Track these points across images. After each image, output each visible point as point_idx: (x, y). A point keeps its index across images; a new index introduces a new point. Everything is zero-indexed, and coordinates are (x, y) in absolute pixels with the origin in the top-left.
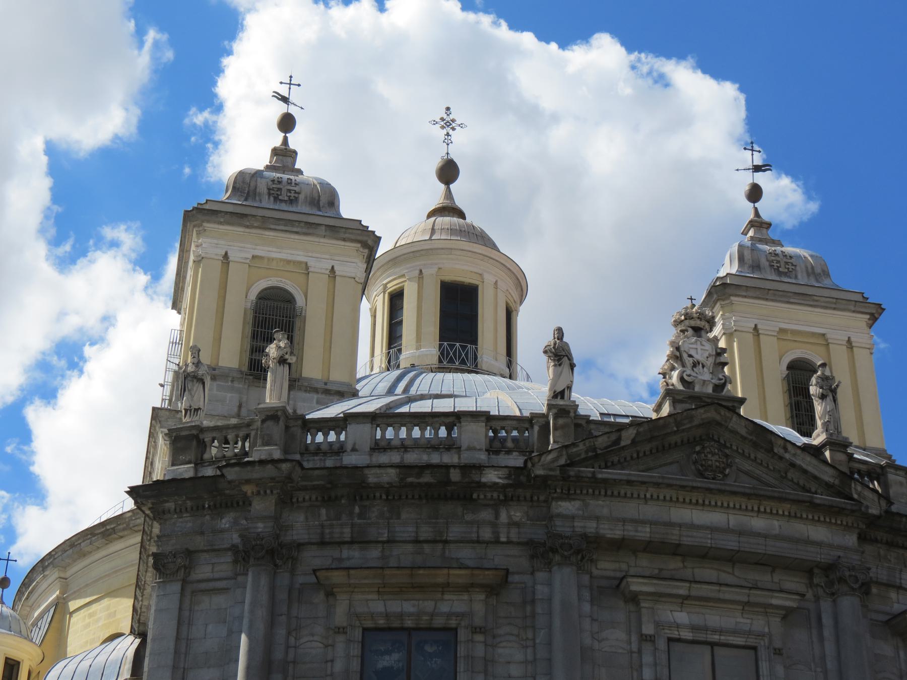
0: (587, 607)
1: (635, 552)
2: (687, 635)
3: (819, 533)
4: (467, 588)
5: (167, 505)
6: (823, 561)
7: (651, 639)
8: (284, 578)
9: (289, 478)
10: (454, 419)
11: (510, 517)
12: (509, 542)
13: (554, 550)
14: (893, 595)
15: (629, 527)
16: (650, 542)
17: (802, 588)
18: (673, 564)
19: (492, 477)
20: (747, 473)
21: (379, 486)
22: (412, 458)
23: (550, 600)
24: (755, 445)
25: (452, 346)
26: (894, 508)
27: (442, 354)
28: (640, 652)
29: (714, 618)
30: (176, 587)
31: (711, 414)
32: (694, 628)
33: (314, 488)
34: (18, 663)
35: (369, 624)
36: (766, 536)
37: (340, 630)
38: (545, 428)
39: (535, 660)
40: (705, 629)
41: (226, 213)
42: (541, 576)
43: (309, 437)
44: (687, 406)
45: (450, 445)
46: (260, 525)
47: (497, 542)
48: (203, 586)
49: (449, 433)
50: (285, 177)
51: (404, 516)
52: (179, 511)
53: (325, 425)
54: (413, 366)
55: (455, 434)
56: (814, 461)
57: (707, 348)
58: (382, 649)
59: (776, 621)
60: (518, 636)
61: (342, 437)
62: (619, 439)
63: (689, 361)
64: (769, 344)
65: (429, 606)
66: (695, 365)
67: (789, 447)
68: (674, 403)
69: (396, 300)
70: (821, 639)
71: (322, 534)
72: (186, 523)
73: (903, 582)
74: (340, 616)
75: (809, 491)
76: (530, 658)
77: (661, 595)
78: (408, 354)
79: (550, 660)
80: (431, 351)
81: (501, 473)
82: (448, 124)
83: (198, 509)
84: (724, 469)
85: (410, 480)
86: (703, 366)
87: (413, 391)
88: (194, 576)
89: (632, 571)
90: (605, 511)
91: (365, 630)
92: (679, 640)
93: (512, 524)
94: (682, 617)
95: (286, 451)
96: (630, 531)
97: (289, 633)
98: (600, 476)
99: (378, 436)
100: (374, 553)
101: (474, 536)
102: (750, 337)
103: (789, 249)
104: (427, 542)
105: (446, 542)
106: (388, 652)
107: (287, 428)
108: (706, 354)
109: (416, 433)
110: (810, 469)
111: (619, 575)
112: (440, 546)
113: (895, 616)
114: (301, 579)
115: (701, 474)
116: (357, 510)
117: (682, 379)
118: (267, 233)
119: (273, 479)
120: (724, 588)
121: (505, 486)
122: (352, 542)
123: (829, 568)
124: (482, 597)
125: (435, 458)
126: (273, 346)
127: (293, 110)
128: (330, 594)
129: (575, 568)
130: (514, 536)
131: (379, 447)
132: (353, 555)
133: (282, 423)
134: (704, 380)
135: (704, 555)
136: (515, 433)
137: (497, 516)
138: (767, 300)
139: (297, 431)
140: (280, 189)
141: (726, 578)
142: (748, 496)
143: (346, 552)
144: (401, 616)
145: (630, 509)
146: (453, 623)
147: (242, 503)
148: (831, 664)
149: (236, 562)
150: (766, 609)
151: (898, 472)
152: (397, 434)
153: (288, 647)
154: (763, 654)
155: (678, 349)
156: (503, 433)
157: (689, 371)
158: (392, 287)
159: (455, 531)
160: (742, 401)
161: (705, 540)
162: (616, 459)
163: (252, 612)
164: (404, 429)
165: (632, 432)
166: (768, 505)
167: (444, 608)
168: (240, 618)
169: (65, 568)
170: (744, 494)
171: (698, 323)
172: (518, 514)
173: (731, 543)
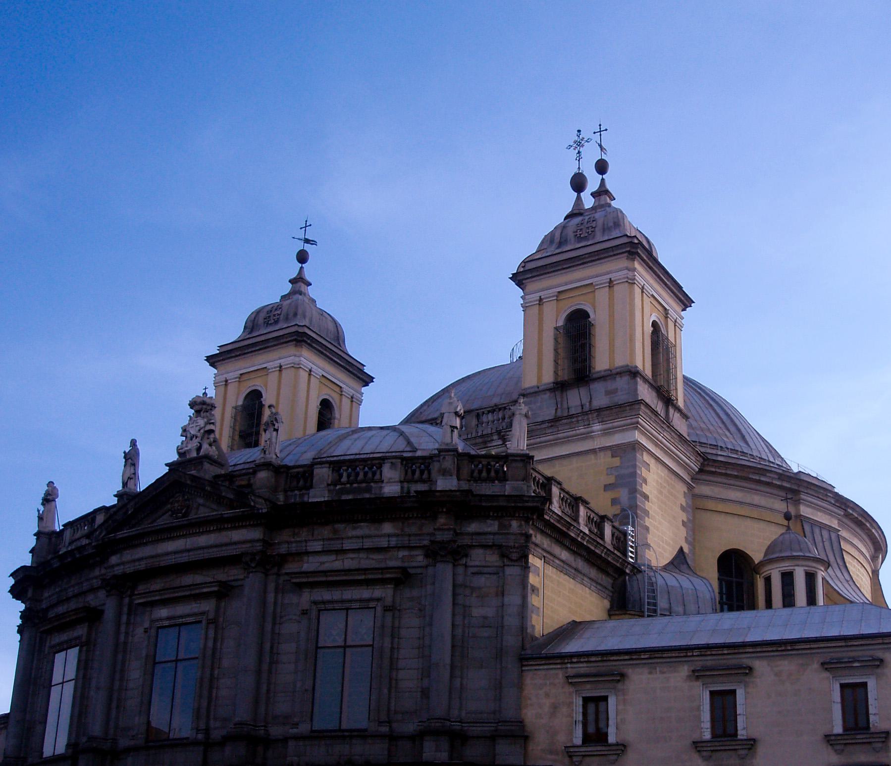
0: (124, 618)
2: (166, 623)
6: (237, 553)
14: (306, 558)
15: (137, 564)
29: (181, 609)
32: (169, 618)
57: (199, 424)
62: (127, 511)
73: (308, 548)
84: (182, 509)
86: (196, 437)
107: (50, 539)
108: (198, 428)
151: (323, 466)
171: (197, 408)
173: (184, 558)
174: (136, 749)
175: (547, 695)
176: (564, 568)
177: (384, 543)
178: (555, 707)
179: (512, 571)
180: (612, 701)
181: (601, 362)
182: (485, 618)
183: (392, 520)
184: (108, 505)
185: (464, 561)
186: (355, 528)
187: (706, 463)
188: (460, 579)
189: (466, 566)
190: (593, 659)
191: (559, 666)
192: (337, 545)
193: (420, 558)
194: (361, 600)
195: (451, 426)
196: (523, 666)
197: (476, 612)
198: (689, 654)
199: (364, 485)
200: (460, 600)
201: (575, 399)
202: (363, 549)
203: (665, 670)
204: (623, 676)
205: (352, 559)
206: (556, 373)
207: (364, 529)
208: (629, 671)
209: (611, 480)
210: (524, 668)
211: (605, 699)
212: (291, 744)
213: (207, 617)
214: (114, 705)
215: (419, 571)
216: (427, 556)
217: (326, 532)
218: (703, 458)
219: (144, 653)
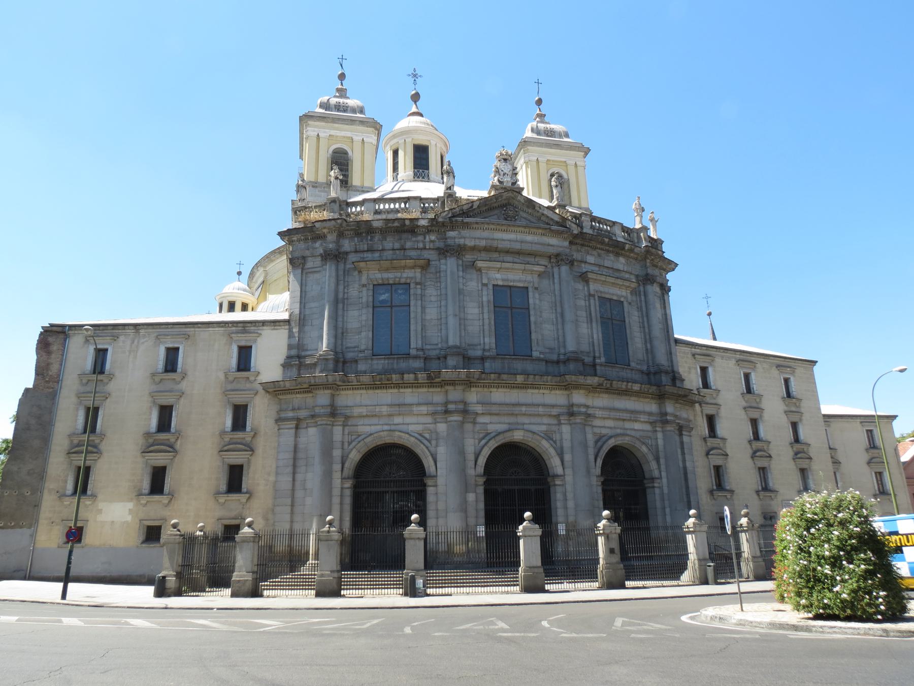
0: (461, 274)
1: (480, 251)
2: (500, 283)
3: (554, 241)
4: (413, 267)
5: (294, 239)
7: (486, 285)
8: (341, 266)
9: (341, 224)
10: (407, 200)
11: (430, 239)
12: (430, 249)
13: (447, 251)
14: (583, 265)
15: (477, 241)
16: (485, 247)
17: (546, 263)
18: (495, 255)
19: (423, 223)
20: (525, 218)
21: (377, 228)
22: (390, 216)
23: (446, 271)
24: (528, 207)
25: (418, 171)
26: (585, 231)
27: (415, 175)
28: (482, 290)
30: (300, 271)
31: (510, 194)
32: (503, 280)
33: (351, 230)
34: (247, 304)
35: (375, 283)
36: (532, 243)
37: (364, 286)
38: (443, 203)
39: (441, 294)
40: (507, 280)
41: (317, 117)
42: (443, 261)
43: (349, 209)
44: (501, 191)
45: (405, 210)
46: (331, 245)
47: (425, 248)
48: (310, 270)
49: (405, 206)
50: (341, 100)
51: (388, 239)
52: (299, 240)
53: (355, 204)
54: (403, 180)
55: (407, 206)
56: (551, 212)
58: (381, 292)
59: (536, 278)
60: (434, 285)
61: (363, 209)
62: (472, 207)
63: (502, 173)
64: (543, 166)
65: (399, 275)
66: (504, 175)
67: (542, 207)
68: (496, 189)
69: (396, 153)
70: (554, 283)
71: (356, 248)
72: (302, 245)
74: (364, 280)
75: (549, 225)
76: (439, 294)
77: (490, 268)
78: (402, 174)
79: (446, 294)
80: (410, 173)
81: (426, 221)
82: (415, 76)
83: (306, 239)
85: (389, 225)
87: (394, 190)
88: (306, 267)
89: (479, 259)
90: (468, 235)
91: (374, 285)
92: (497, 285)
93: (431, 241)
94: (498, 276)
95: (341, 214)
96: (478, 243)
97: (344, 288)
98: (465, 221)
99: (377, 208)
100: (377, 255)
101: (416, 247)
102: (535, 163)
103: (552, 126)
104: (397, 250)
105: (405, 249)
106: (384, 294)
107: (340, 205)
109: (392, 206)
110: (549, 215)
111: (473, 260)
112: (403, 251)
113: (583, 274)
114: (348, 266)
115: (506, 219)
116: (369, 238)
117: (499, 181)
118: (335, 125)
119: (335, 227)
120: (515, 264)
121: (428, 226)
122: (368, 251)
123: (557, 255)
124: (420, 270)
125: (400, 215)
126: (333, 172)
128: (360, 272)
129: (455, 258)
130: (432, 246)
131: (377, 212)
132: (369, 255)
133: (338, 204)
134: (507, 180)
135: (508, 252)
136: (432, 205)
137: (425, 238)
138: (542, 147)
139: (344, 207)
140: (340, 106)
141: (516, 260)
142: (525, 227)
143: (366, 255)
144: (388, 279)
145: (478, 233)
146: (408, 281)
147: (322, 237)
148: (557, 292)
149: (322, 260)
150: (532, 272)
152: (384, 207)
153: (344, 293)
154: (530, 290)
155: (497, 168)
156: (427, 205)
157: (501, 177)
158: (394, 147)
159: (409, 245)
160: (523, 189)
161: (507, 245)
162: (472, 214)
163: (329, 280)
164: (397, 204)
165: (478, 203)
166: (533, 230)
167: (405, 275)
168: (325, 282)
169: (265, 267)
170: (523, 227)
171: (506, 157)
172: (433, 238)
173: (517, 246)
174: (493, 358)
175: (686, 362)
177: (621, 267)
178: (690, 368)
180: (710, 370)
183: (622, 255)
184: (423, 196)
186: (608, 256)
190: (703, 348)
192: (600, 262)
194: (617, 295)
196: (676, 345)
199: (607, 233)
202: (612, 268)
205: (606, 272)
207: (612, 257)
210: (677, 347)
212: (598, 367)
213: (533, 285)
214: (462, 327)
217: (595, 253)
219: (485, 299)
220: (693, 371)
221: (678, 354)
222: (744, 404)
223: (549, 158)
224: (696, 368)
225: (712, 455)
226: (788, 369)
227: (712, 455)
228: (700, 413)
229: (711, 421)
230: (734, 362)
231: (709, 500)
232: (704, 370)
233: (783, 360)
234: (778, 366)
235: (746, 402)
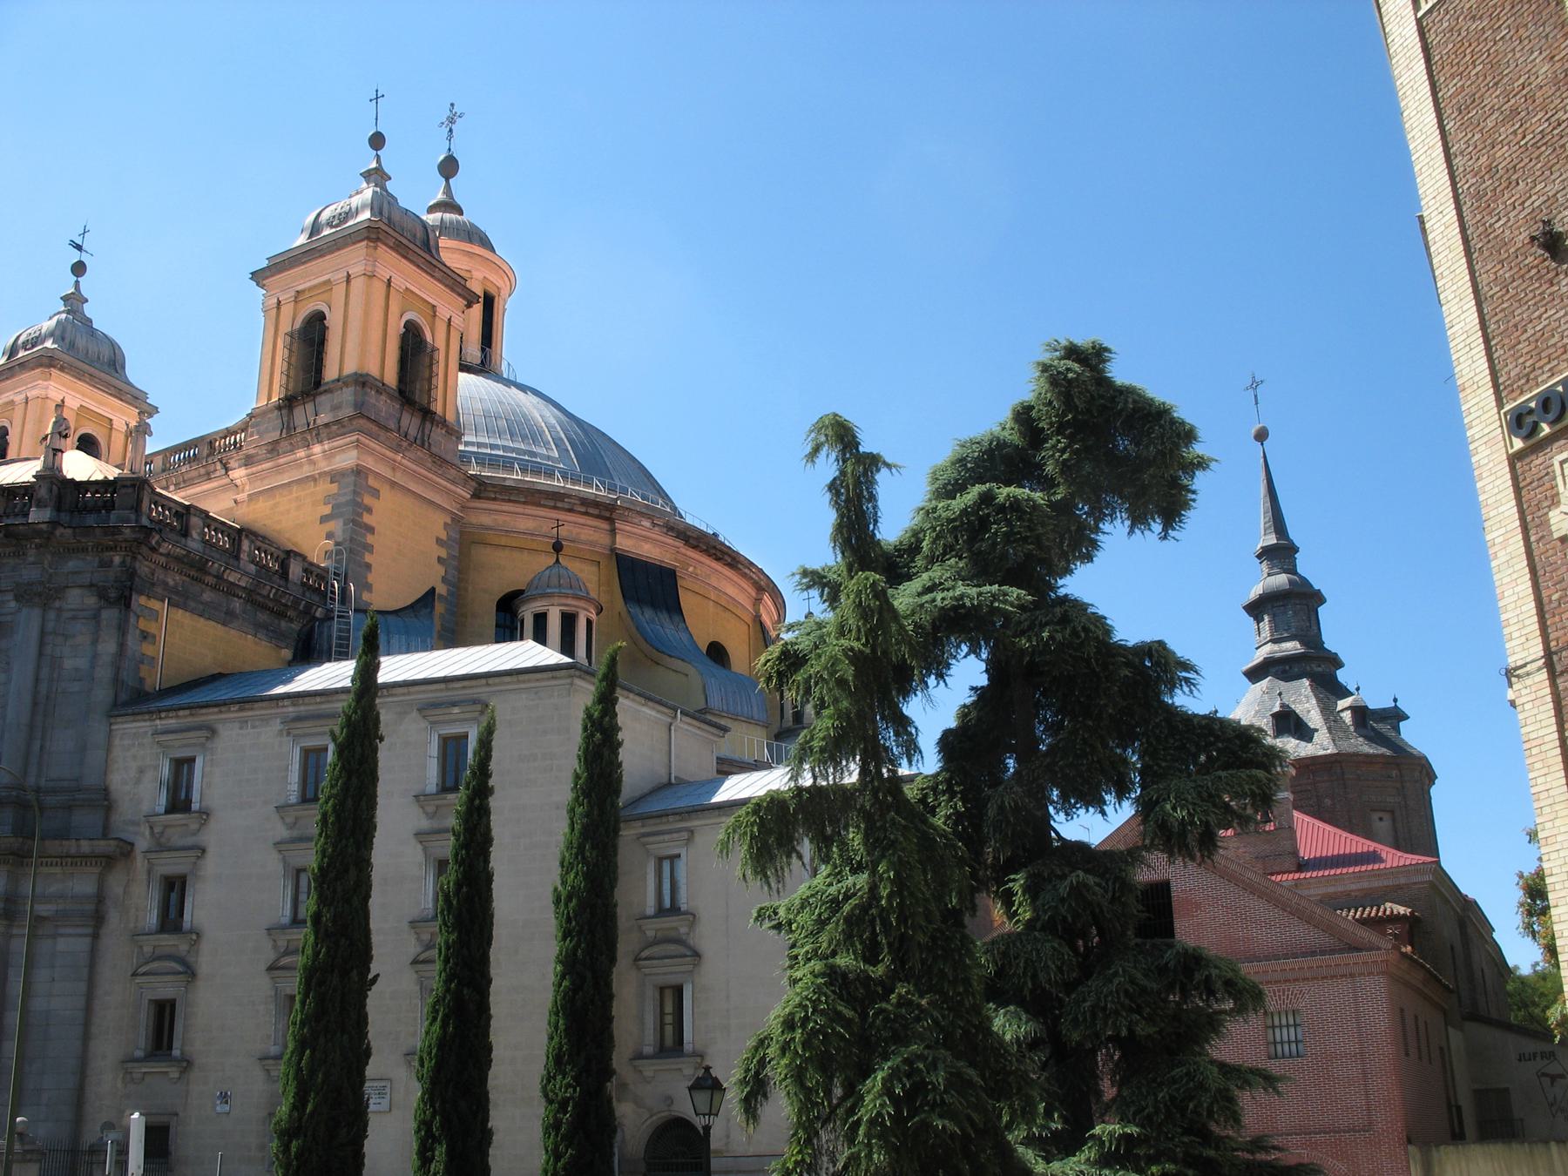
127: (85, 258)
175: (135, 757)
176: (206, 612)
178: (141, 771)
179: (110, 615)
181: (331, 373)
182: (77, 670)
185: (57, 604)
187: (483, 488)
188: (50, 626)
189: (60, 610)
190: (181, 713)
191: (148, 723)
193: (13, 604)
195: (53, 449)
196: (111, 724)
197: (68, 664)
198: (280, 704)
200: (48, 650)
201: (300, 415)
203: (257, 723)
204: (212, 731)
206: (287, 389)
208: (220, 727)
209: (327, 510)
211: (192, 760)
215: (9, 618)
216: (17, 598)
218: (477, 483)
220: (149, 775)
221: (117, 742)
222: (283, 832)
223: (300, 288)
224: (156, 767)
225: (144, 974)
226: (456, 710)
227: (144, 974)
228: (145, 877)
229: (174, 889)
230: (276, 726)
231: (119, 1084)
232: (183, 766)
233: (443, 686)
234: (425, 709)
235: (291, 827)
